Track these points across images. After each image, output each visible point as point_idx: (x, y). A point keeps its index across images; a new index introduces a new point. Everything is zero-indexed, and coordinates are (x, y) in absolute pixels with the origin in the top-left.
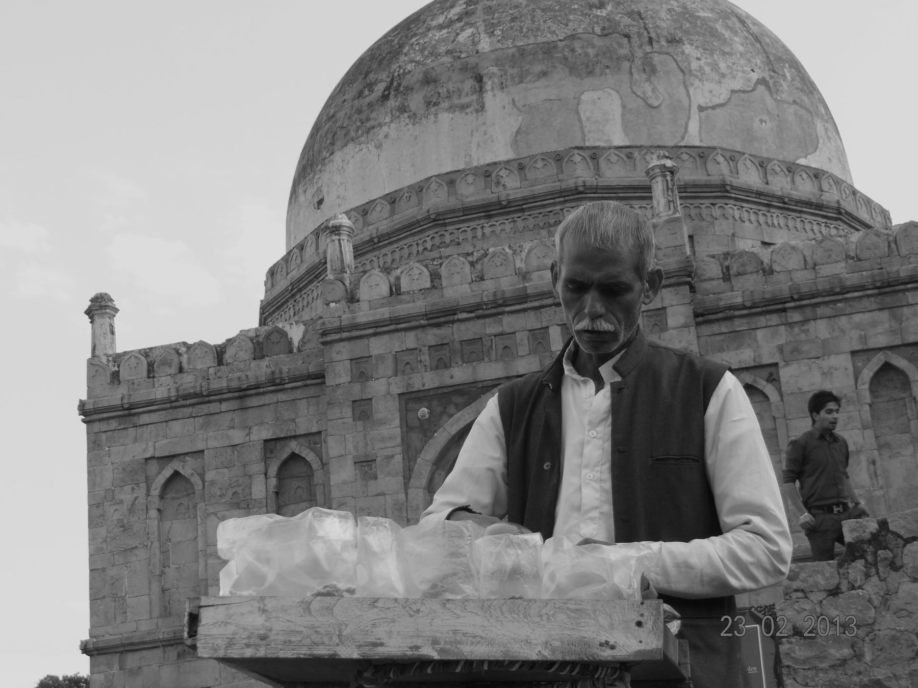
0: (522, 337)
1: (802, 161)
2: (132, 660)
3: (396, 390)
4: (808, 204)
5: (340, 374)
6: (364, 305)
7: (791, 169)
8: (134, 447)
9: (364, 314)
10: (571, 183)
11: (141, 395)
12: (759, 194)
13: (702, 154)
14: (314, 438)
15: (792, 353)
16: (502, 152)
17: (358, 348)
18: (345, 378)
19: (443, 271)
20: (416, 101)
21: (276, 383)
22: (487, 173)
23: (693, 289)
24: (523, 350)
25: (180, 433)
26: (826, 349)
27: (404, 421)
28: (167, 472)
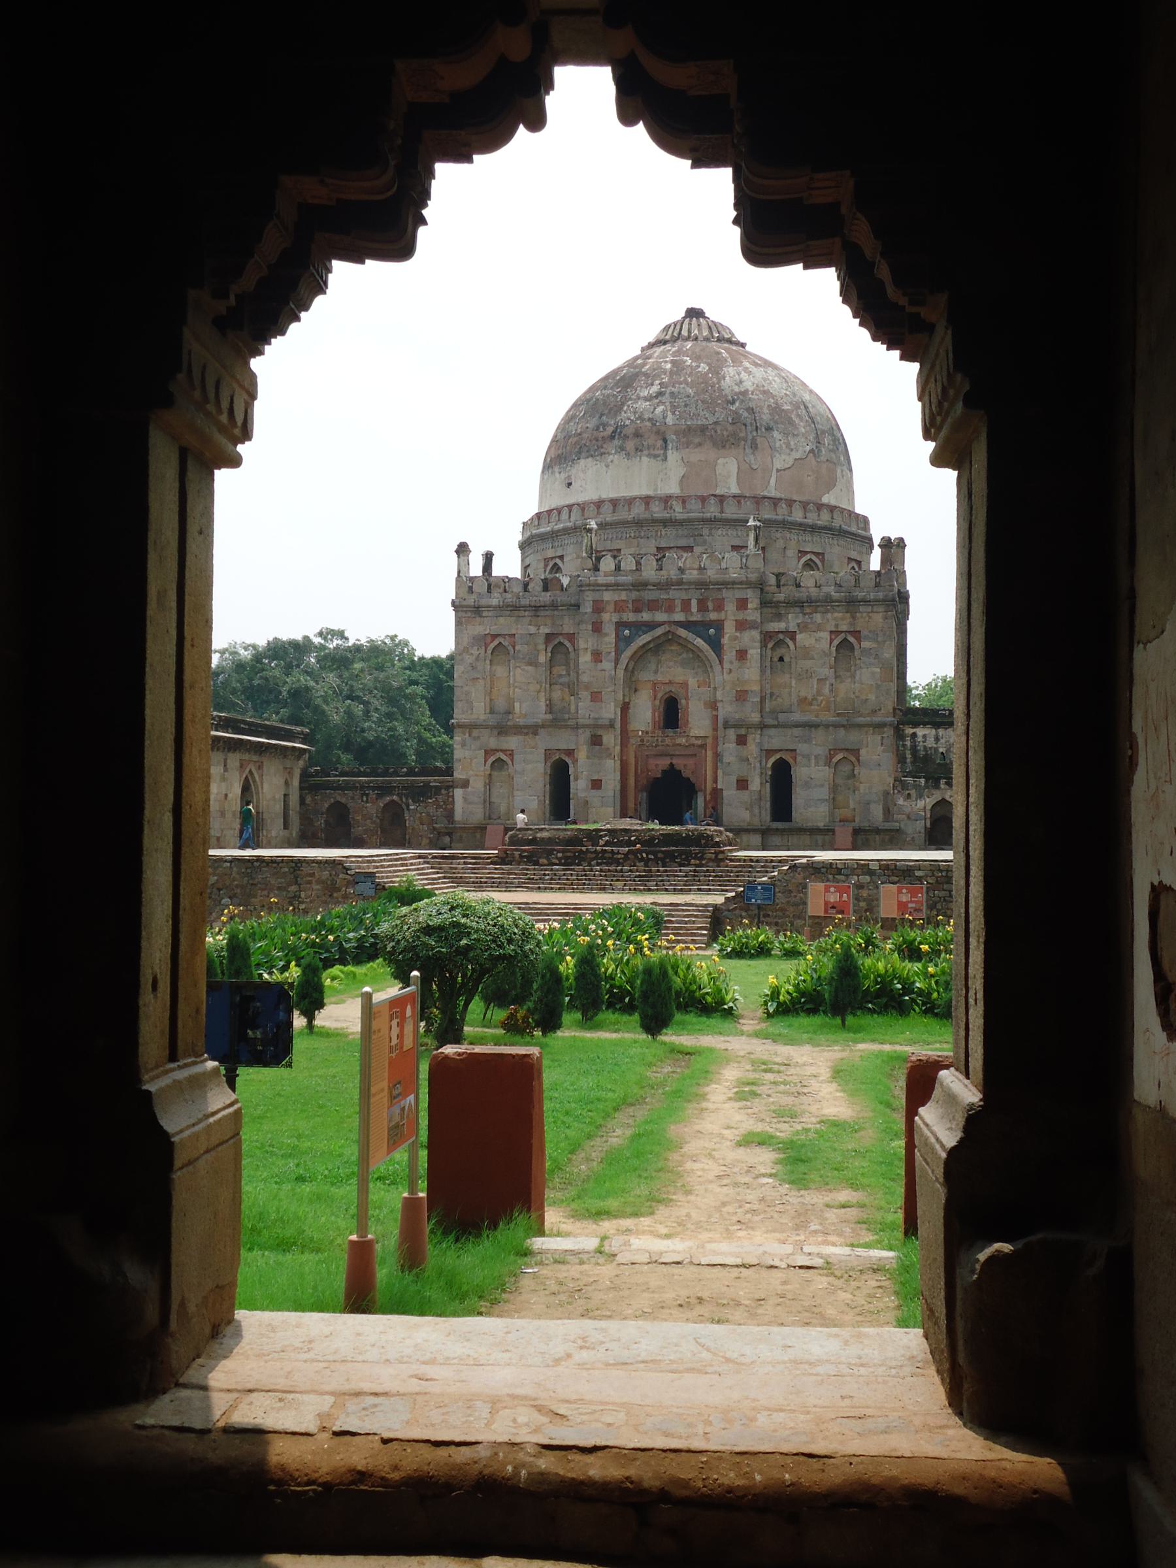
0: (678, 602)
1: (825, 499)
2: (475, 733)
3: (614, 620)
4: (825, 528)
5: (587, 608)
6: (601, 573)
7: (820, 507)
8: (479, 628)
9: (601, 579)
10: (708, 515)
11: (483, 602)
12: (801, 525)
13: (775, 502)
14: (571, 637)
15: (803, 627)
16: (673, 489)
17: (597, 596)
18: (589, 610)
19: (643, 561)
20: (630, 445)
21: (554, 606)
22: (666, 500)
23: (762, 590)
24: (678, 609)
25: (504, 624)
26: (819, 628)
27: (617, 635)
28: (496, 643)
